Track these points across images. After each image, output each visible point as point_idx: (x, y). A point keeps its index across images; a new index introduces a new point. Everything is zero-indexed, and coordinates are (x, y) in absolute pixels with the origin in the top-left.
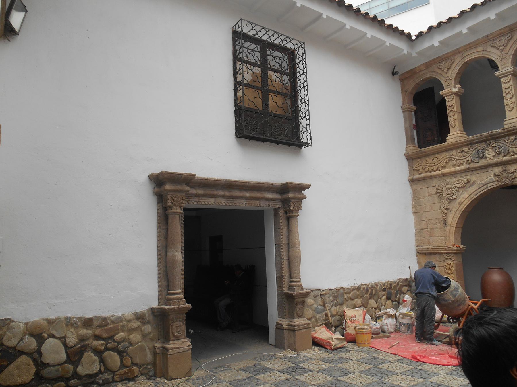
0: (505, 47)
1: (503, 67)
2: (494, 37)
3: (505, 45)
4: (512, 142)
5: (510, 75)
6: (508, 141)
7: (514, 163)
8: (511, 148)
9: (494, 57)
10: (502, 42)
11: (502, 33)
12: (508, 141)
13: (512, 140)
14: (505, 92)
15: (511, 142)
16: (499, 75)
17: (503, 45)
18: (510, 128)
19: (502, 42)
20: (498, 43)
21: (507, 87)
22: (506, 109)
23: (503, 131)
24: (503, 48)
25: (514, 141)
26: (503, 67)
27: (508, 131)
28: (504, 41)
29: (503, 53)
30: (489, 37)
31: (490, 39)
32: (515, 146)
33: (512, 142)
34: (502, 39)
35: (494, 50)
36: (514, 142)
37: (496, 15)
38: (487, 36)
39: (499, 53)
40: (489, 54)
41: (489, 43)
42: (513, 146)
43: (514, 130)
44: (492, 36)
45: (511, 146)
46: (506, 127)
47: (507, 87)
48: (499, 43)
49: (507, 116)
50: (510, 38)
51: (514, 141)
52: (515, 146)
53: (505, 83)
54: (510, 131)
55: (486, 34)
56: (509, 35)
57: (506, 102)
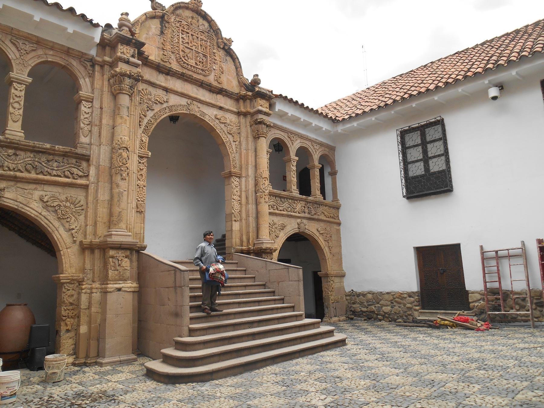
0: (26, 54)
1: (19, 72)
2: (19, 35)
3: (28, 52)
4: (10, 156)
5: (24, 84)
6: (5, 153)
7: (4, 180)
8: (6, 162)
9: (10, 55)
10: (26, 47)
11: (28, 38)
12: (5, 153)
13: (11, 154)
14: (14, 99)
15: (8, 155)
16: (13, 78)
17: (25, 51)
18: (14, 141)
19: (26, 47)
20: (21, 44)
21: (18, 95)
22: (10, 118)
23: (5, 140)
24: (24, 54)
25: (11, 156)
26: (19, 72)
27: (11, 143)
28: (28, 47)
29: (22, 57)
30: (14, 32)
31: (13, 34)
32: (12, 162)
33: (10, 156)
34: (27, 44)
35: (14, 49)
36: (12, 157)
37: (41, 19)
38: (12, 29)
39: (18, 56)
40: (6, 47)
41: (9, 37)
42: (9, 161)
43: (17, 144)
44: (17, 33)
45: (7, 160)
46: (7, 136)
47: (18, 95)
48: (22, 46)
49: (8, 125)
50: (35, 49)
51: (11, 156)
52: (12, 162)
53: (16, 90)
54: (14, 143)
55: (12, 26)
56: (35, 45)
57: (11, 110)
